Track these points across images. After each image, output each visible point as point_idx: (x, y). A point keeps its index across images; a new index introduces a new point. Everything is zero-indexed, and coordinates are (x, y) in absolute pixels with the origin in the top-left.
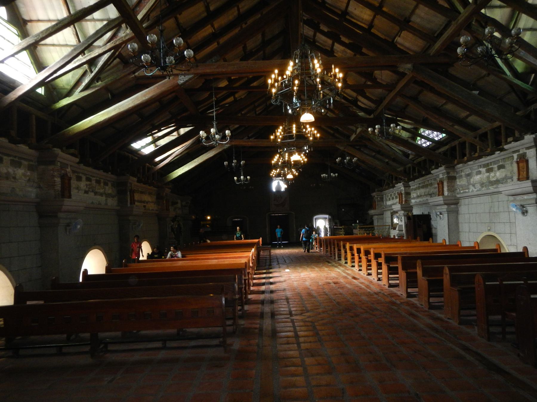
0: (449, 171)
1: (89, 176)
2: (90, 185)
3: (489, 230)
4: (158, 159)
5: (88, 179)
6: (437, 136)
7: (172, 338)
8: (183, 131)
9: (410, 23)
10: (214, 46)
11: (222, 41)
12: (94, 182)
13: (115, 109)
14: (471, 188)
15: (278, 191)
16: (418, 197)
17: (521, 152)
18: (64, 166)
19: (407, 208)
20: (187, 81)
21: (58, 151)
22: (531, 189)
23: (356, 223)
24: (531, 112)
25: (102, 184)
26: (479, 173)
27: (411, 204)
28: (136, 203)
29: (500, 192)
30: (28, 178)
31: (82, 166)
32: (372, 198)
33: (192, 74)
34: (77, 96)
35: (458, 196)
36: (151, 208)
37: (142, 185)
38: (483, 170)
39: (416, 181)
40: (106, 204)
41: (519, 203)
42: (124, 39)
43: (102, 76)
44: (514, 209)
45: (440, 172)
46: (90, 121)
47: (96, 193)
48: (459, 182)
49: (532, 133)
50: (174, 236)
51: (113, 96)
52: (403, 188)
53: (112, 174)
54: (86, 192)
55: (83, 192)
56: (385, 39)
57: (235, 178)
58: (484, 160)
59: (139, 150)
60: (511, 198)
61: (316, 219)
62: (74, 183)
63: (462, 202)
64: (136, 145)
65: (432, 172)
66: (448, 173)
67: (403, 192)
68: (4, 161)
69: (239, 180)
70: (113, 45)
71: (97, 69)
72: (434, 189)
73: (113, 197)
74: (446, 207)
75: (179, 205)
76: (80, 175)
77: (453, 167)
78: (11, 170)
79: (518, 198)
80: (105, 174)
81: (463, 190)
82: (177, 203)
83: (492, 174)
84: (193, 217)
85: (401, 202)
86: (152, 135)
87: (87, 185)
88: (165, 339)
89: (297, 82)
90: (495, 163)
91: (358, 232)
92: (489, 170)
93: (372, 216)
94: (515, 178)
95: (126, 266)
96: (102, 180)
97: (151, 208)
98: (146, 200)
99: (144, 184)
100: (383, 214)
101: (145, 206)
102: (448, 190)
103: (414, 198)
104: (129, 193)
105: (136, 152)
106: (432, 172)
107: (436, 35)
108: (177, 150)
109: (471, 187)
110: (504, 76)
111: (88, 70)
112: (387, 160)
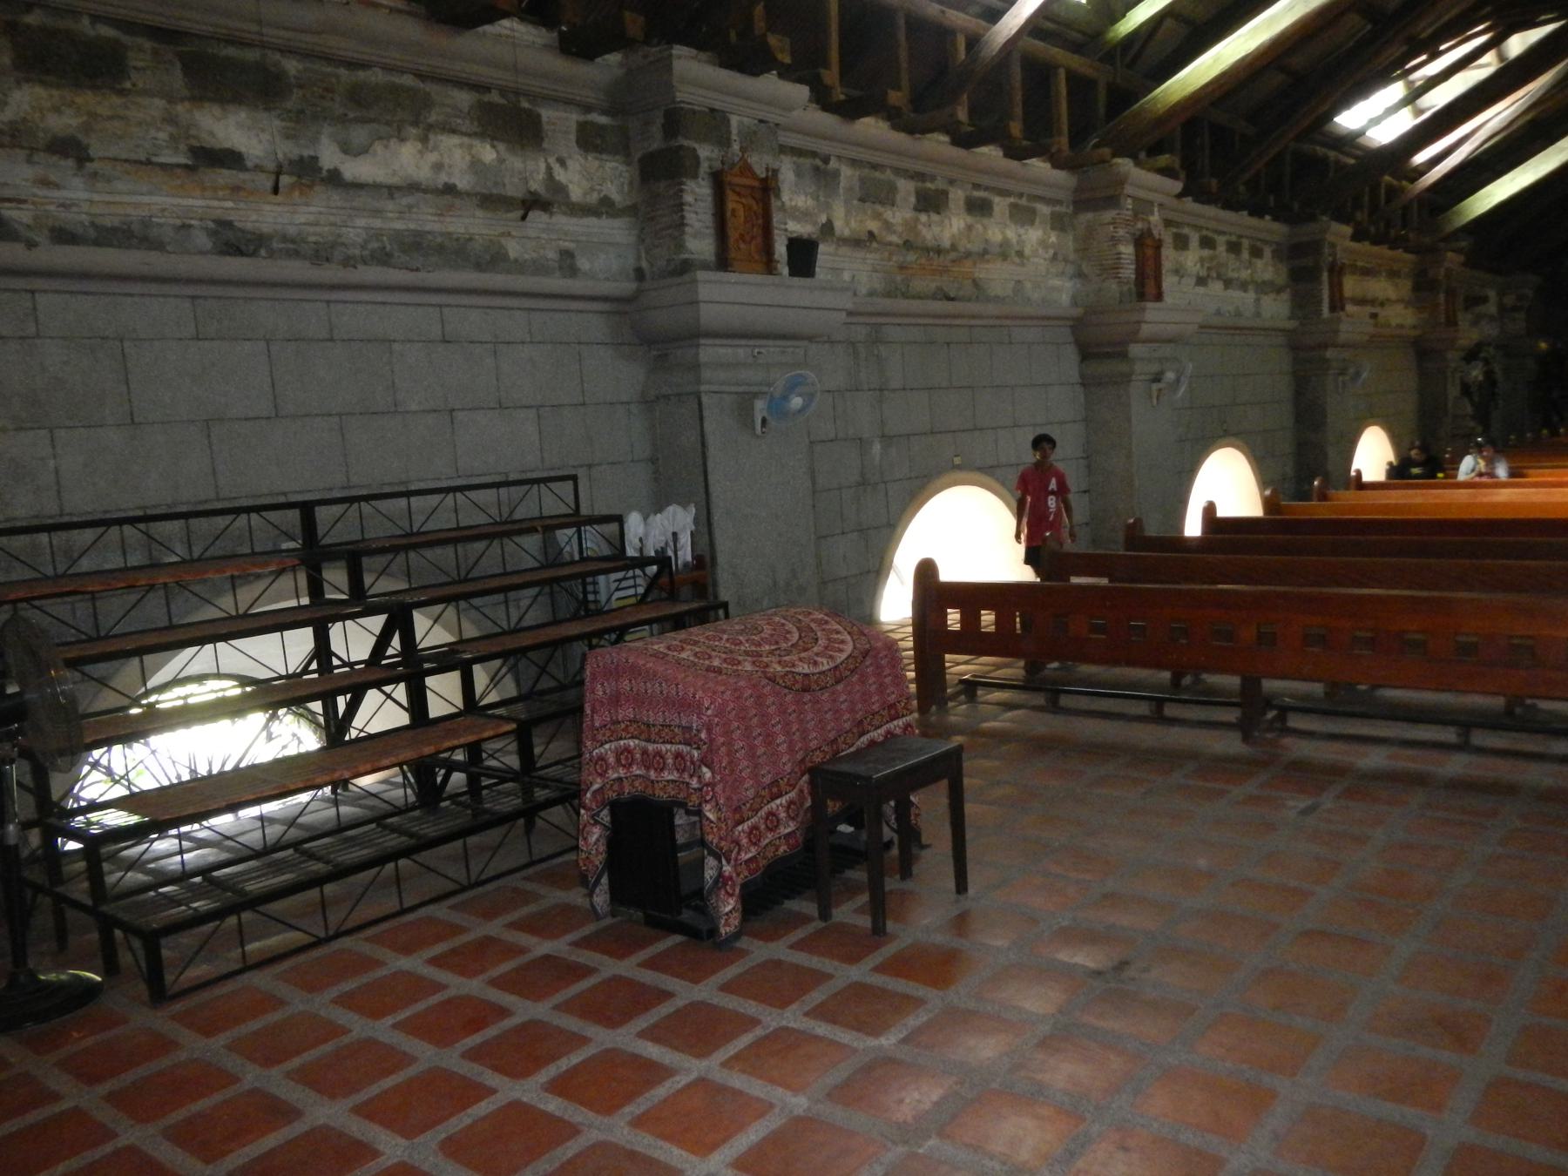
1: (1210, 234)
2: (1212, 259)
4: (1420, 158)
5: (1207, 243)
8: (1517, 44)
12: (1221, 249)
18: (1142, 207)
21: (1125, 164)
25: (1245, 255)
28: (1350, 308)
30: (1051, 252)
31: (1189, 204)
36: (1394, 322)
37: (1366, 246)
40: (1258, 314)
47: (1228, 284)
50: (1469, 410)
53: (1276, 219)
54: (1201, 281)
55: (1194, 280)
59: (1361, 133)
62: (1169, 255)
64: (1349, 119)
68: (996, 209)
73: (1279, 291)
75: (1491, 308)
76: (1186, 231)
78: (1011, 234)
80: (1254, 221)
82: (1485, 300)
84: (1543, 345)
87: (1202, 260)
88: (1467, 722)
95: (1323, 497)
96: (1246, 243)
97: (1394, 322)
98: (1379, 298)
99: (1375, 243)
101: (1374, 316)
104: (1325, 275)
105: (1350, 141)
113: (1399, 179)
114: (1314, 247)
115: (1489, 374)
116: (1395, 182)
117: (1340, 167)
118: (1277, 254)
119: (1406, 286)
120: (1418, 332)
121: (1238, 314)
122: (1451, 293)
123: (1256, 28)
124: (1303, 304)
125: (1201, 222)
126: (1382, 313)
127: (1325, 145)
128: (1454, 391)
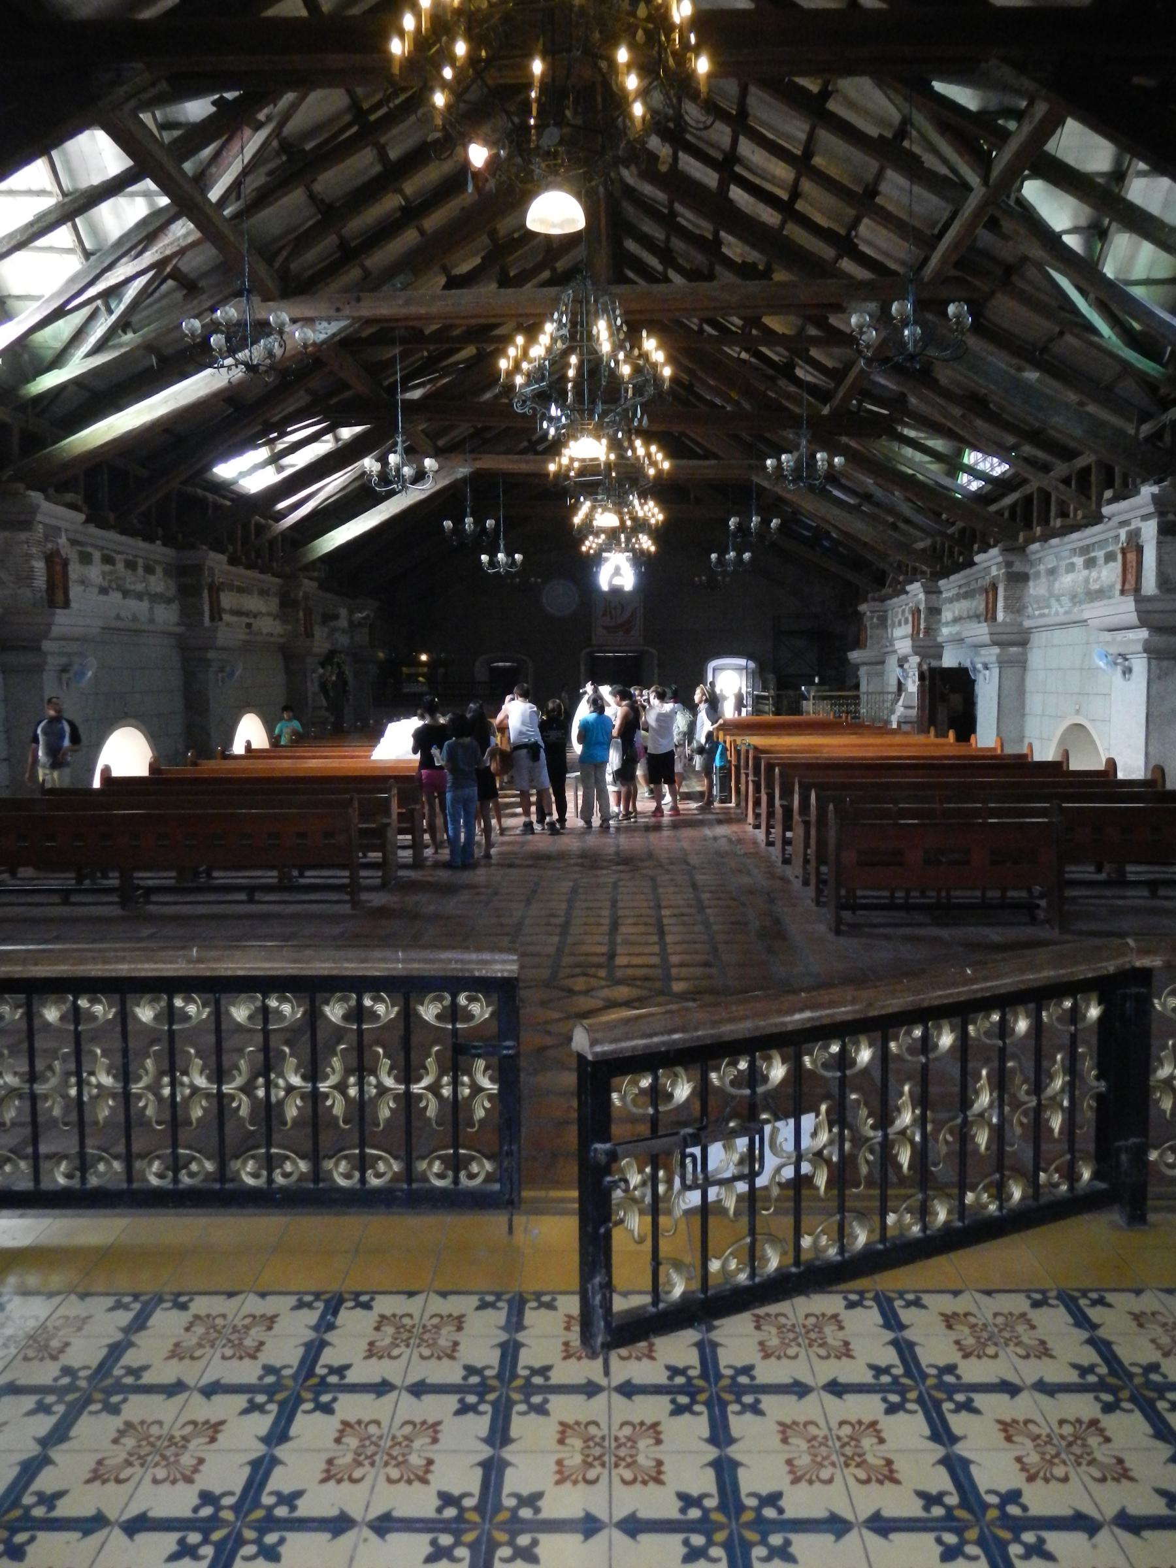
0: (1011, 558)
2: (111, 573)
3: (1078, 712)
4: (281, 506)
5: (108, 560)
6: (997, 467)
7: (269, 889)
8: (346, 433)
9: (878, 200)
10: (409, 238)
11: (434, 221)
12: (120, 566)
13: (166, 401)
14: (1055, 605)
15: (616, 591)
16: (956, 620)
17: (1133, 527)
18: (52, 532)
19: (928, 647)
20: (334, 335)
21: (36, 496)
22: (1133, 618)
23: (813, 683)
24: (1164, 426)
25: (140, 571)
26: (1071, 568)
27: (939, 639)
28: (226, 617)
29: (1083, 622)
31: (92, 529)
32: (859, 616)
33: (348, 317)
34: (76, 367)
35: (1027, 623)
36: (265, 631)
37: (241, 570)
38: (1079, 561)
39: (952, 578)
40: (152, 621)
41: (1114, 650)
42: (183, 243)
43: (135, 319)
44: (1101, 664)
45: (990, 561)
46: (110, 428)
47: (126, 594)
48: (1036, 589)
49: (1156, 483)
50: (325, 703)
51: (163, 360)
52: (922, 596)
53: (164, 545)
54: (103, 591)
55: (96, 590)
56: (829, 229)
57: (484, 558)
58: (1076, 539)
59: (235, 482)
60: (1108, 636)
61: (714, 670)
62: (75, 570)
63: (1037, 639)
64: (225, 470)
65: (977, 559)
66: (1009, 564)
67: (922, 607)
69: (493, 563)
70: (157, 257)
71: (122, 307)
72: (978, 604)
73: (169, 601)
74: (996, 650)
75: (343, 623)
76: (89, 549)
77: (1022, 550)
79: (1120, 636)
81: (1040, 608)
82: (336, 617)
83: (1094, 574)
84: (381, 655)
85: (914, 636)
86: (271, 442)
87: (104, 573)
88: (251, 890)
89: (574, 360)
90: (1102, 543)
91: (812, 709)
92: (1090, 563)
93: (857, 667)
94: (1118, 587)
95: (195, 764)
96: (140, 562)
97: (265, 631)
98: (250, 609)
99: (248, 567)
100: (883, 662)
101: (249, 626)
102: (1006, 608)
103: (947, 624)
104: (206, 594)
105: (223, 488)
106: (977, 559)
107: (936, 231)
108: (333, 484)
109: (1053, 602)
110: (1096, 339)
111: (103, 308)
112: (891, 520)
113: (266, 518)
114: (197, 569)
115: (341, 675)
116: (262, 521)
117: (218, 507)
118: (167, 573)
119: (273, 604)
120: (281, 640)
121: (135, 618)
122: (308, 612)
123: (139, 412)
124: (190, 614)
125: (101, 543)
126: (258, 624)
127: (205, 489)
128: (313, 687)
